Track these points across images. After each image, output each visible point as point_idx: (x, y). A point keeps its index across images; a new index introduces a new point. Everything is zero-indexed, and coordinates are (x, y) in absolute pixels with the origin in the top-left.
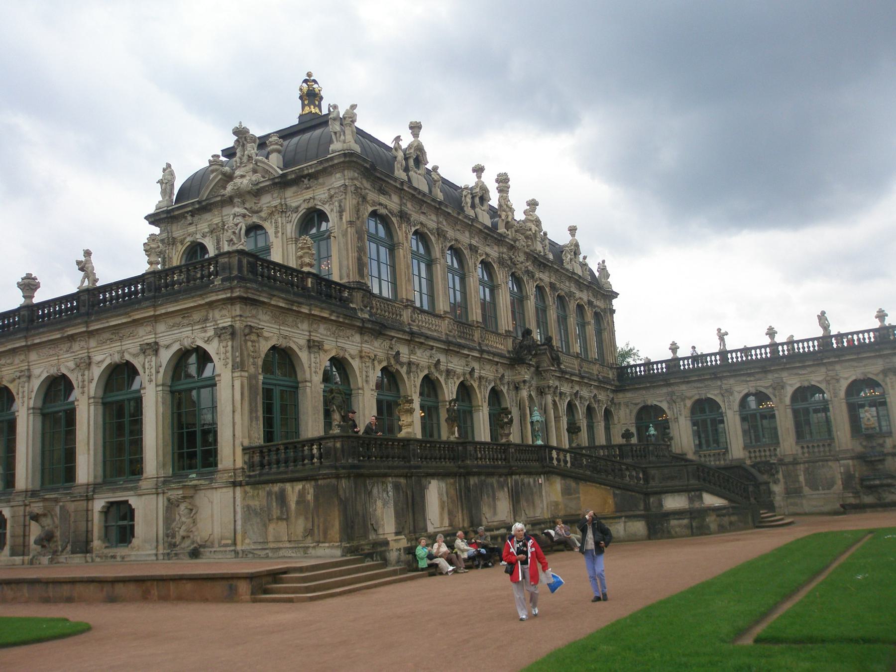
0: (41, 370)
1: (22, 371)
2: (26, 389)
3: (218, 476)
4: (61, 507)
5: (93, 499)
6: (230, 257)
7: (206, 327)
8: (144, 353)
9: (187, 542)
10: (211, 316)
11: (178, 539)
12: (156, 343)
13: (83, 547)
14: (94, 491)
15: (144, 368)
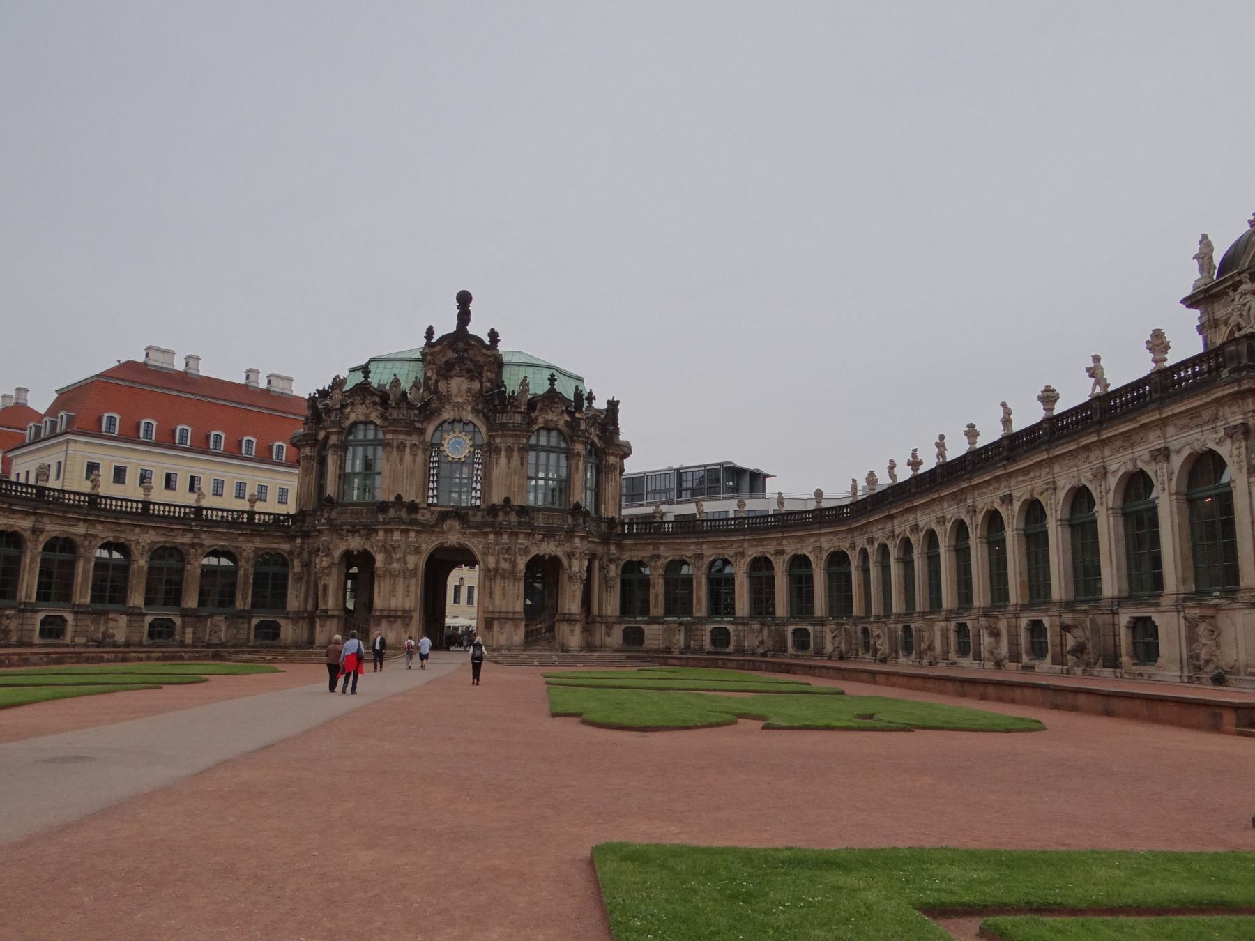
0: (1064, 481)
1: (1048, 484)
2: (1053, 501)
3: (1240, 595)
4: (1090, 619)
5: (1118, 614)
6: (1237, 345)
7: (1216, 427)
8: (1155, 459)
9: (1210, 667)
10: (1221, 414)
11: (1202, 662)
12: (1166, 449)
13: (1113, 661)
14: (1119, 605)
15: (1156, 475)
